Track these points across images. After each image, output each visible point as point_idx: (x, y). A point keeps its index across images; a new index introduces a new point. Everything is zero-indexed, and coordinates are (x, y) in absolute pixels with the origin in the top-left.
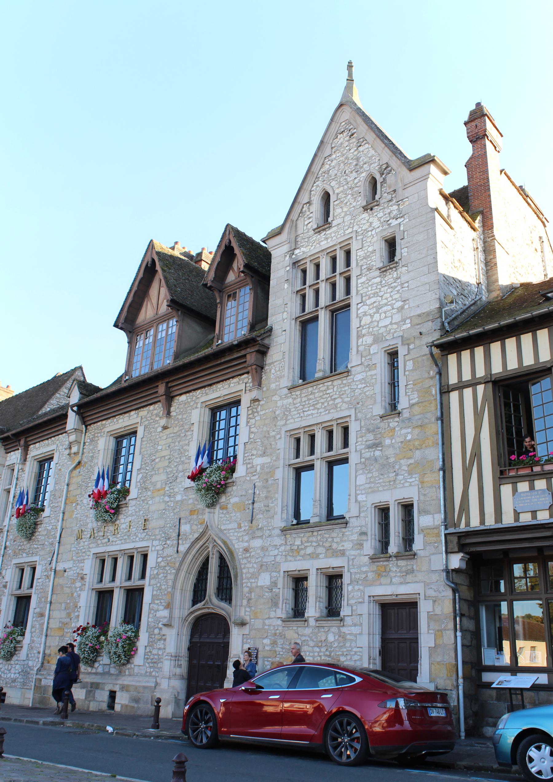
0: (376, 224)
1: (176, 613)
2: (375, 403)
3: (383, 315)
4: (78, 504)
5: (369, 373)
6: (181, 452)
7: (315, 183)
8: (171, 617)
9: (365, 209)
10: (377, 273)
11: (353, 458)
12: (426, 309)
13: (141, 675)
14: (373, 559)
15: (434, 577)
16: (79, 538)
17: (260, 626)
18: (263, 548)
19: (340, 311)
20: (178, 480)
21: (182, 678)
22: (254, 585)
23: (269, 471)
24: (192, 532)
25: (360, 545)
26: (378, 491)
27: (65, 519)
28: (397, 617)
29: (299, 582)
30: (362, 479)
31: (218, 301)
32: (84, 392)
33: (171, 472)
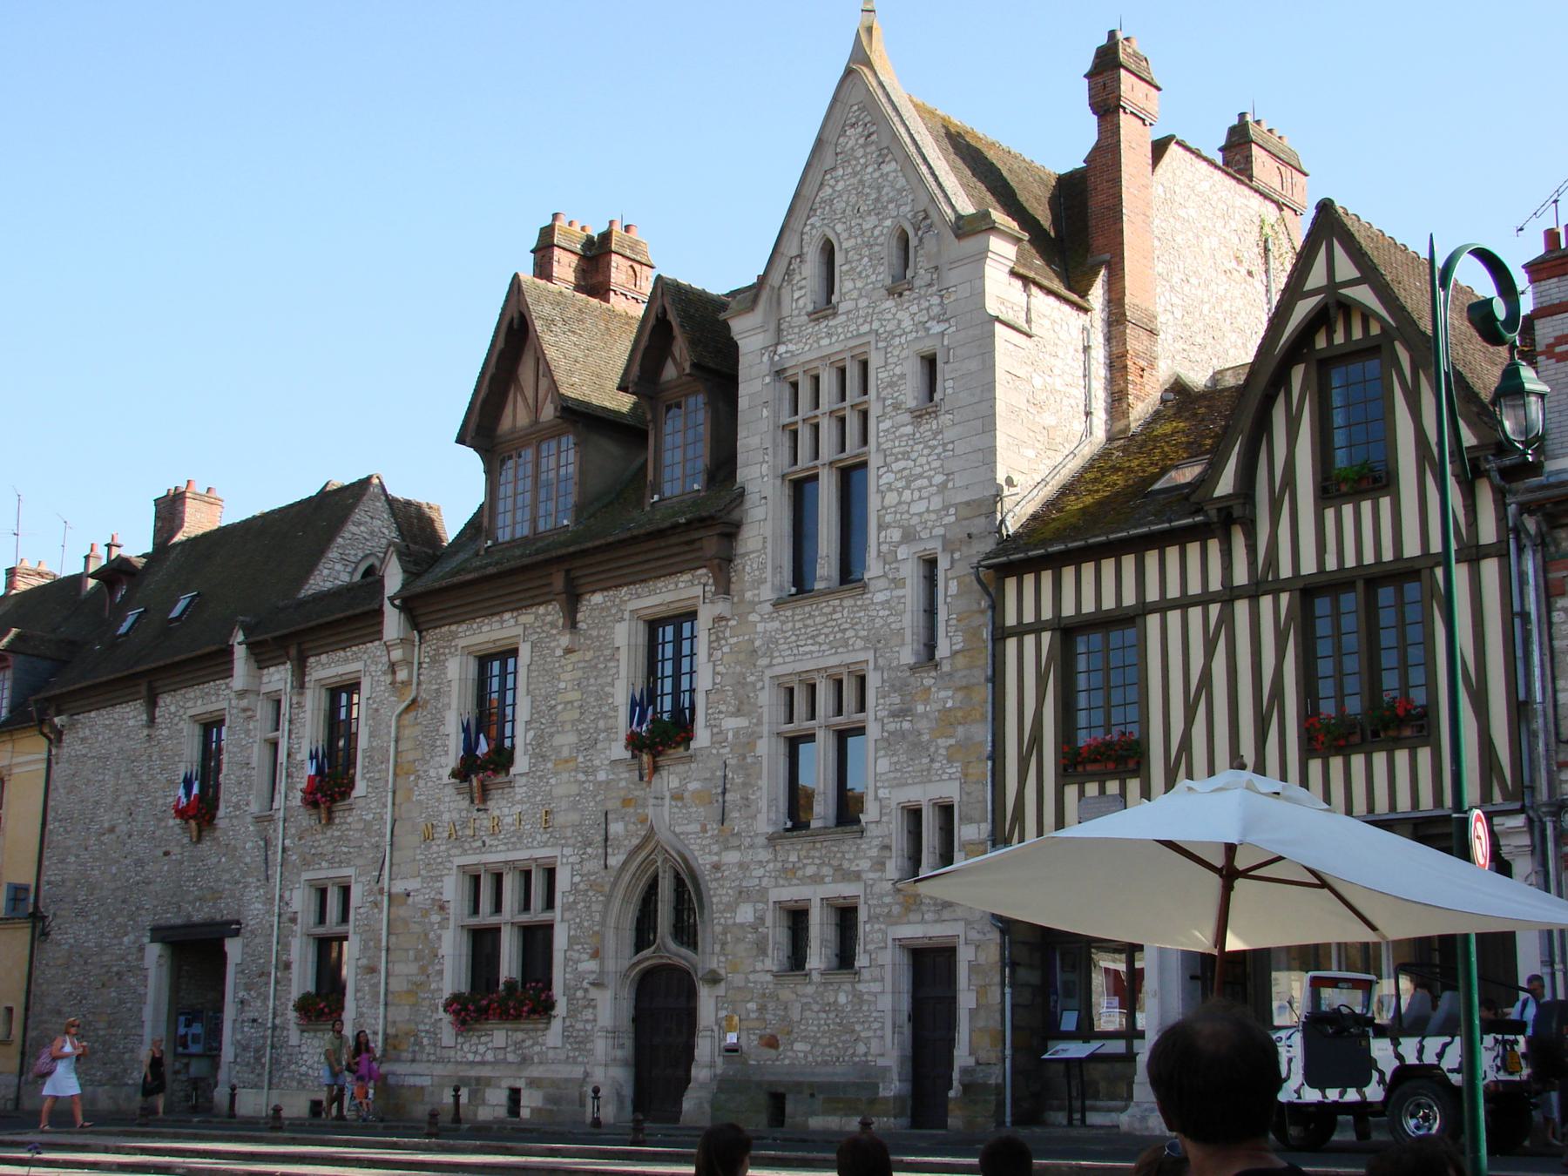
0: (907, 324)
1: (610, 965)
2: (903, 644)
4: (419, 777)
5: (895, 593)
6: (603, 696)
7: (808, 218)
8: (602, 972)
10: (906, 418)
11: (873, 730)
16: (428, 838)
17: (742, 984)
18: (742, 866)
19: (851, 477)
20: (599, 746)
21: (625, 1063)
23: (747, 741)
25: (880, 865)
26: (906, 784)
29: (797, 918)
30: (883, 765)
31: (649, 417)
32: (414, 569)
33: (586, 731)
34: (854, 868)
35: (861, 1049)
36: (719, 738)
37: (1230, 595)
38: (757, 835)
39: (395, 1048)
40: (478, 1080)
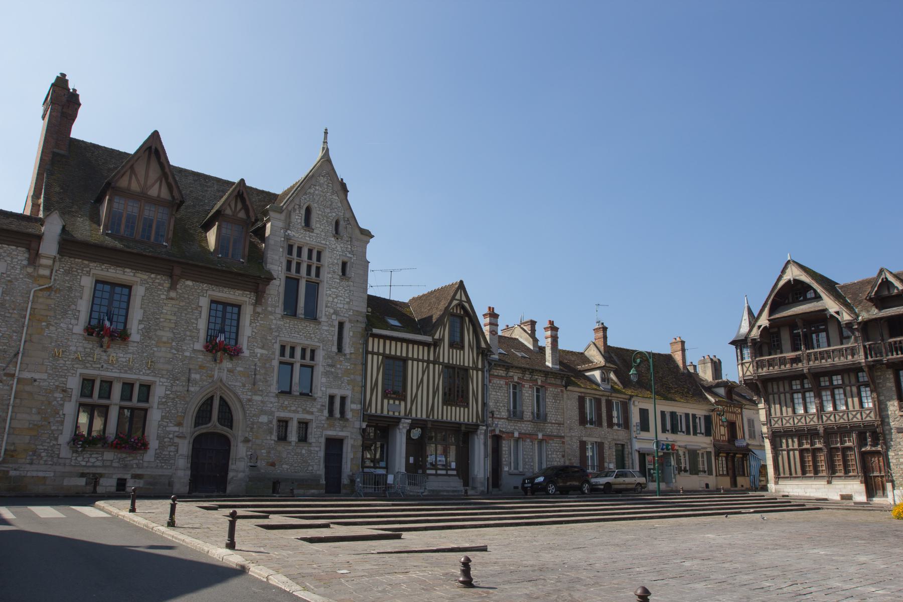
0: (339, 248)
11: (319, 370)
12: (359, 309)
14: (327, 419)
18: (262, 402)
25: (321, 411)
28: (334, 446)
29: (284, 424)
30: (324, 380)
33: (179, 334)
35: (310, 468)
37: (428, 362)
39: (12, 456)
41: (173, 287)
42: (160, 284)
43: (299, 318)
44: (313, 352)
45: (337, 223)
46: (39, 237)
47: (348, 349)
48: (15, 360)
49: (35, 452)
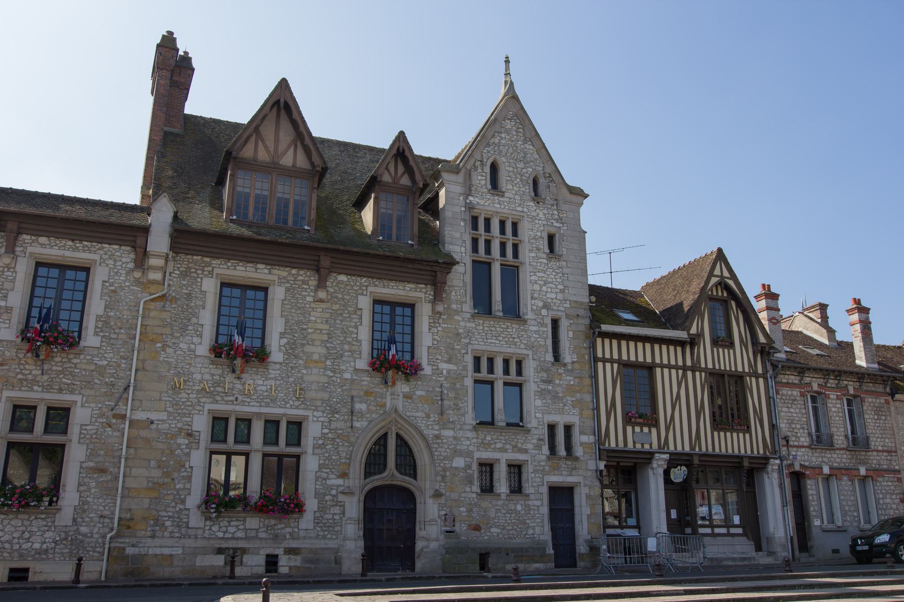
0: (541, 215)
2: (547, 351)
3: (549, 290)
9: (534, 200)
10: (545, 256)
11: (531, 388)
13: (311, 538)
14: (549, 458)
15: (589, 473)
17: (457, 498)
18: (455, 438)
20: (344, 359)
22: (448, 466)
24: (369, 411)
25: (538, 447)
27: (141, 357)
29: (487, 468)
30: (539, 403)
33: (335, 348)
34: (524, 447)
35: (531, 531)
36: (438, 372)
38: (465, 424)
39: (129, 527)
40: (235, 550)
41: (322, 284)
42: (304, 282)
43: (496, 317)
44: (519, 363)
45: (535, 182)
46: (145, 230)
47: (568, 356)
48: (125, 395)
49: (157, 521)
